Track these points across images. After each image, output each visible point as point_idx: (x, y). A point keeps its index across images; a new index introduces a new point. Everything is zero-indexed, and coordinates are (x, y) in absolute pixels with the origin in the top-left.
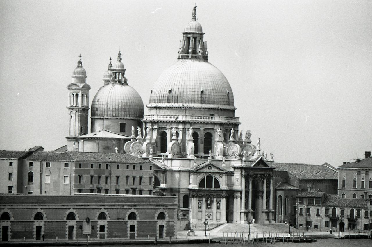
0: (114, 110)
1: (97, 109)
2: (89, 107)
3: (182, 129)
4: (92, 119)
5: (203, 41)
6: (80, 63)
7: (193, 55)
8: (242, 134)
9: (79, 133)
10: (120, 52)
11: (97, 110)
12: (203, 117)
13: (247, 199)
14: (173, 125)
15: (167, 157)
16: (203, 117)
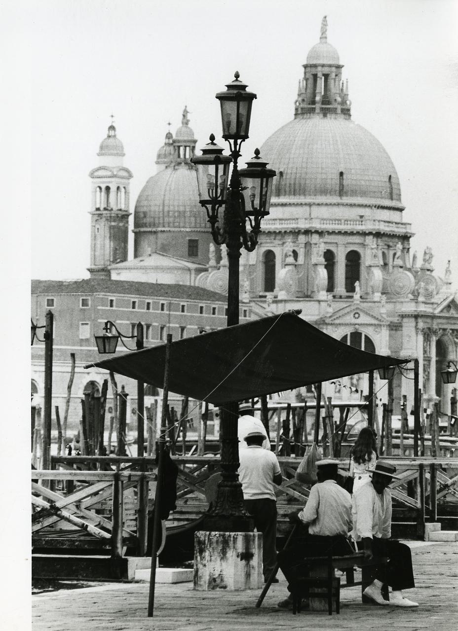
0: (176, 214)
1: (145, 213)
2: (130, 212)
3: (304, 245)
4: (136, 233)
5: (341, 82)
6: (112, 128)
7: (324, 106)
8: (416, 257)
9: (112, 260)
10: (186, 107)
11: (145, 217)
12: (343, 221)
13: (426, 376)
14: (286, 237)
15: (276, 297)
16: (343, 221)
